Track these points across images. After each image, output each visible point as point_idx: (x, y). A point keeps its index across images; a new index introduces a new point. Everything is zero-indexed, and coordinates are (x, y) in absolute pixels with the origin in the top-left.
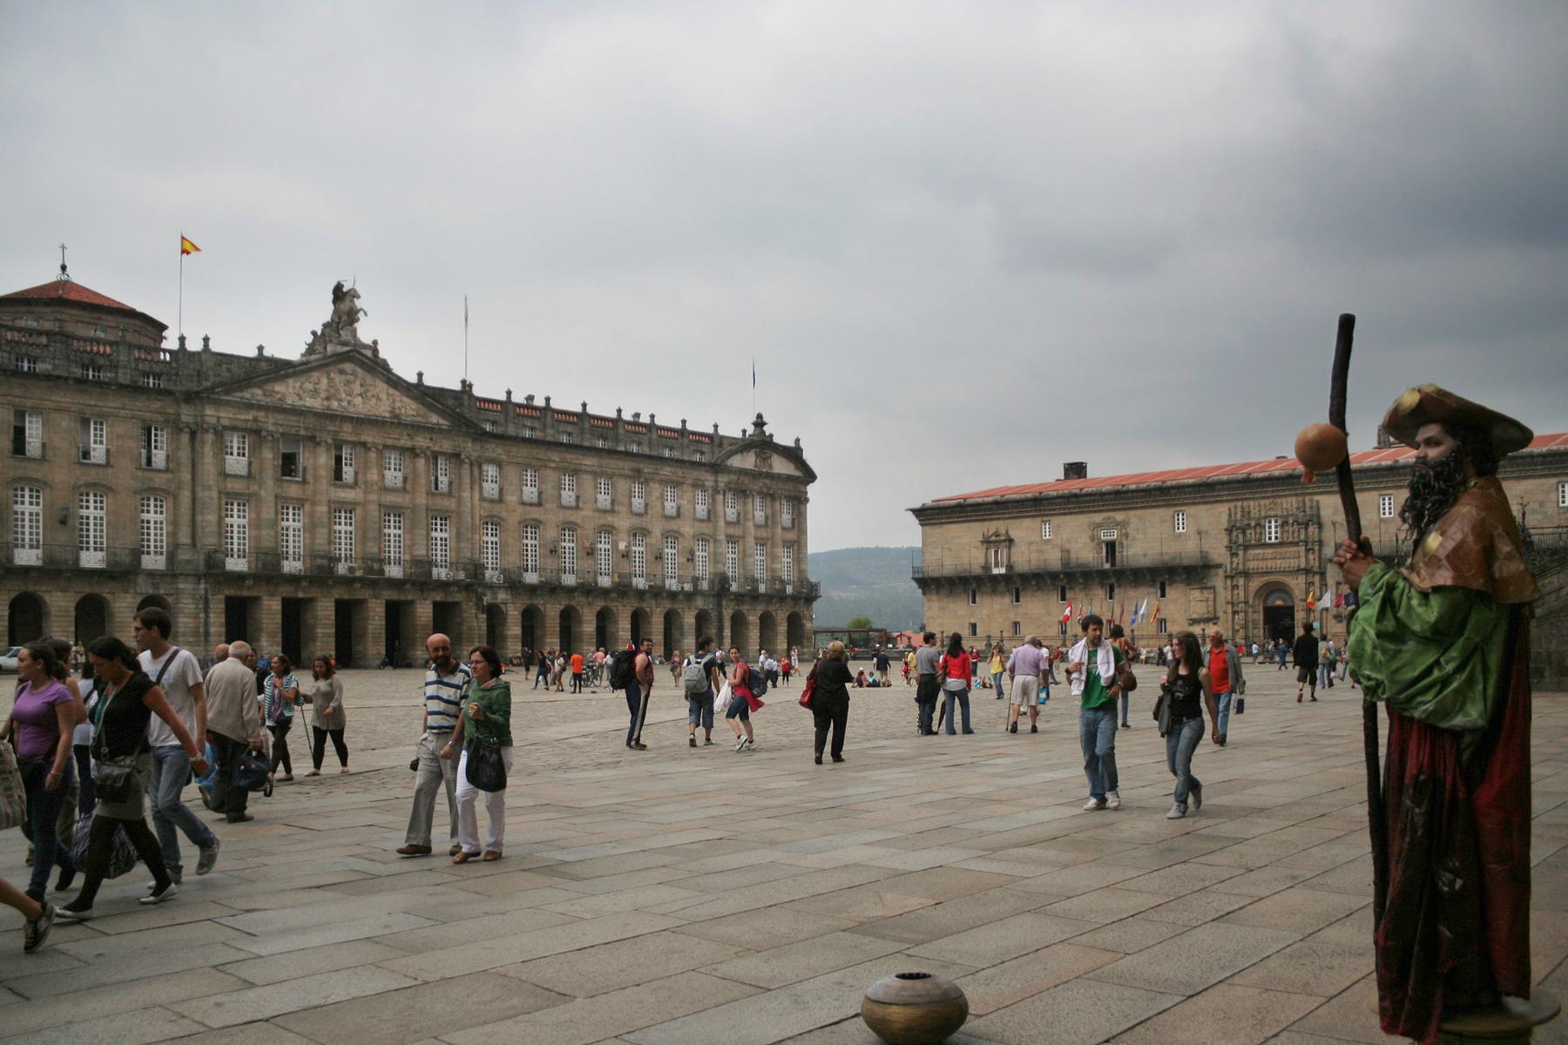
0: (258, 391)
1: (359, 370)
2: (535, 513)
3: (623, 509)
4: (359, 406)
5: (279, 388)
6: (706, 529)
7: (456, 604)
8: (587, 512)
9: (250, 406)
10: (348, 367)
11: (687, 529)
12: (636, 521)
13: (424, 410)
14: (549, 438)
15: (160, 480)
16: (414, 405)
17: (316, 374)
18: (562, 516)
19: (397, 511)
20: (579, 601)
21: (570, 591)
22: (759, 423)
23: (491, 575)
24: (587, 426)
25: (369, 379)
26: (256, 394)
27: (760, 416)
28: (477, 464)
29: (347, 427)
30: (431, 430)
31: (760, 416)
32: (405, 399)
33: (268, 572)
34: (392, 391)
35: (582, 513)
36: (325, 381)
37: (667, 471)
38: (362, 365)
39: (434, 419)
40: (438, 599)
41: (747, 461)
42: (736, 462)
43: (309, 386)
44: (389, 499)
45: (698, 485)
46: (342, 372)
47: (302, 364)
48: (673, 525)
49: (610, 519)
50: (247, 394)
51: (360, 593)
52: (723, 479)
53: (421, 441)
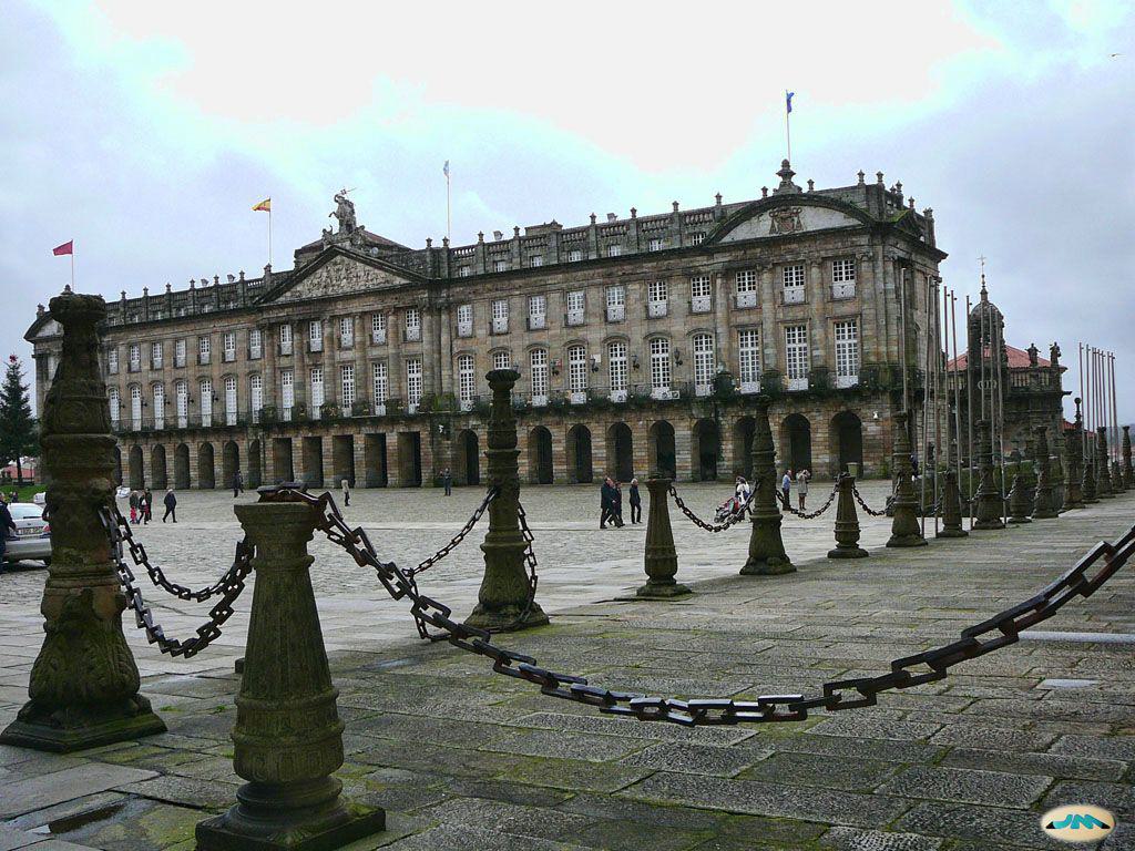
0: (288, 294)
2: (502, 341)
3: (594, 320)
4: (345, 286)
5: (299, 288)
6: (704, 323)
7: (418, 433)
9: (283, 306)
10: (338, 258)
11: (678, 327)
12: (611, 330)
13: (390, 277)
14: (516, 267)
15: (257, 365)
16: (383, 274)
18: (528, 339)
19: (378, 362)
21: (541, 411)
22: (786, 173)
23: (466, 405)
24: (554, 243)
26: (287, 297)
27: (786, 164)
28: (451, 307)
29: (340, 305)
30: (393, 290)
31: (786, 164)
32: (376, 271)
33: (301, 419)
34: (368, 268)
35: (551, 332)
36: (325, 274)
37: (648, 267)
38: (343, 254)
39: (399, 281)
41: (763, 227)
42: (741, 233)
43: (316, 281)
44: (375, 353)
45: (691, 275)
46: (335, 264)
47: (297, 270)
48: (660, 327)
49: (581, 333)
50: (281, 299)
51: (349, 431)
52: (721, 259)
53: (391, 302)
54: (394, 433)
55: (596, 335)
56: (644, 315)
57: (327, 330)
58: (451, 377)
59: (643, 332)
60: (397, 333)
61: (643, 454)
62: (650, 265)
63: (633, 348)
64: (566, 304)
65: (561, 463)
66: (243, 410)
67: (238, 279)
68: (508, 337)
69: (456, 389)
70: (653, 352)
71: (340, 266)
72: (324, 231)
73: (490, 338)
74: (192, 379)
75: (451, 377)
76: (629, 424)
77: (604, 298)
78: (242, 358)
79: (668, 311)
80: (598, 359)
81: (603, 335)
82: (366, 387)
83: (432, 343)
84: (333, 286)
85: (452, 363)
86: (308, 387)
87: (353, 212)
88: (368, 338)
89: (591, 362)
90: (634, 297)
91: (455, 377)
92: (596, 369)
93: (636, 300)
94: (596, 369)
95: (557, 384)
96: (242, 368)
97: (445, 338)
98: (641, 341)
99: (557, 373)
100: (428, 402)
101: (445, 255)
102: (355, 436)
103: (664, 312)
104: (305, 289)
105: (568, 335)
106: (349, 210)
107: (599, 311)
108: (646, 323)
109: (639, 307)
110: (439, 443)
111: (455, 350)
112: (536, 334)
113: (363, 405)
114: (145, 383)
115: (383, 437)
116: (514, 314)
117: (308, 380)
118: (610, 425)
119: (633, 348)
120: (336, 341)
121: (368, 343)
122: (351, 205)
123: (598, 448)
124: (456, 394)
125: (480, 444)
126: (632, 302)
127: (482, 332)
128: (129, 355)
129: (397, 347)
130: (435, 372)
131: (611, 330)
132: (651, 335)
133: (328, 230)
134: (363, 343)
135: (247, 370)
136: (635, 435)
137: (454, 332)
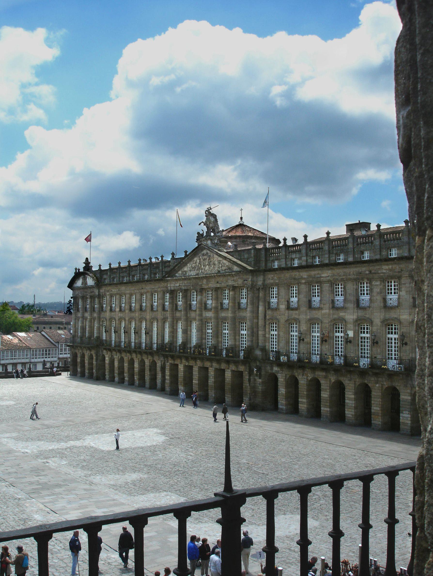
1: (208, 252)
3: (351, 305)
8: (325, 311)
10: (205, 252)
17: (195, 259)
20: (320, 374)
25: (212, 254)
28: (266, 288)
35: (324, 311)
36: (198, 261)
40: (233, 369)
43: (193, 265)
44: (223, 314)
46: (203, 255)
48: (393, 314)
49: (342, 314)
51: (207, 364)
54: (229, 370)
55: (350, 316)
56: (382, 305)
57: (199, 297)
58: (264, 336)
59: (382, 317)
60: (234, 303)
61: (379, 409)
62: (387, 267)
63: (375, 329)
64: (333, 292)
65: (326, 406)
66: (160, 342)
67: (148, 261)
68: (297, 312)
69: (267, 344)
70: (389, 333)
71: (205, 257)
72: (198, 233)
73: (287, 312)
74: (137, 319)
75: (264, 336)
76: (370, 385)
77: (357, 290)
78: (160, 309)
79: (399, 303)
80: (351, 334)
81: (355, 317)
82: (217, 337)
83: (252, 312)
84: (202, 269)
85: (265, 326)
86: (189, 333)
87: (216, 220)
88: (219, 304)
89: (346, 336)
90: (376, 290)
91: (267, 336)
92: (350, 342)
93: (378, 293)
94: (350, 342)
95: (326, 347)
96: (160, 315)
97: (261, 308)
98: (379, 324)
99: (326, 341)
100: (249, 351)
101: (263, 252)
102: (210, 368)
103: (396, 304)
104: (188, 269)
105: (333, 314)
106: (212, 219)
107: (352, 298)
108: (383, 310)
109: (379, 298)
110: (255, 380)
111: (268, 317)
112: (314, 312)
113: (216, 349)
114: (117, 319)
115: (223, 371)
116: (302, 296)
117: (189, 328)
118: (358, 383)
119: (375, 329)
120: (203, 305)
121: (219, 307)
122: (215, 216)
123: (350, 399)
124: (267, 347)
125: (279, 384)
126: (375, 294)
127: (283, 307)
128: (111, 301)
129: (234, 312)
130: (254, 333)
131: (361, 313)
132: (387, 320)
133: (201, 232)
134: (216, 308)
135: (162, 317)
136: (373, 393)
137: (268, 305)
